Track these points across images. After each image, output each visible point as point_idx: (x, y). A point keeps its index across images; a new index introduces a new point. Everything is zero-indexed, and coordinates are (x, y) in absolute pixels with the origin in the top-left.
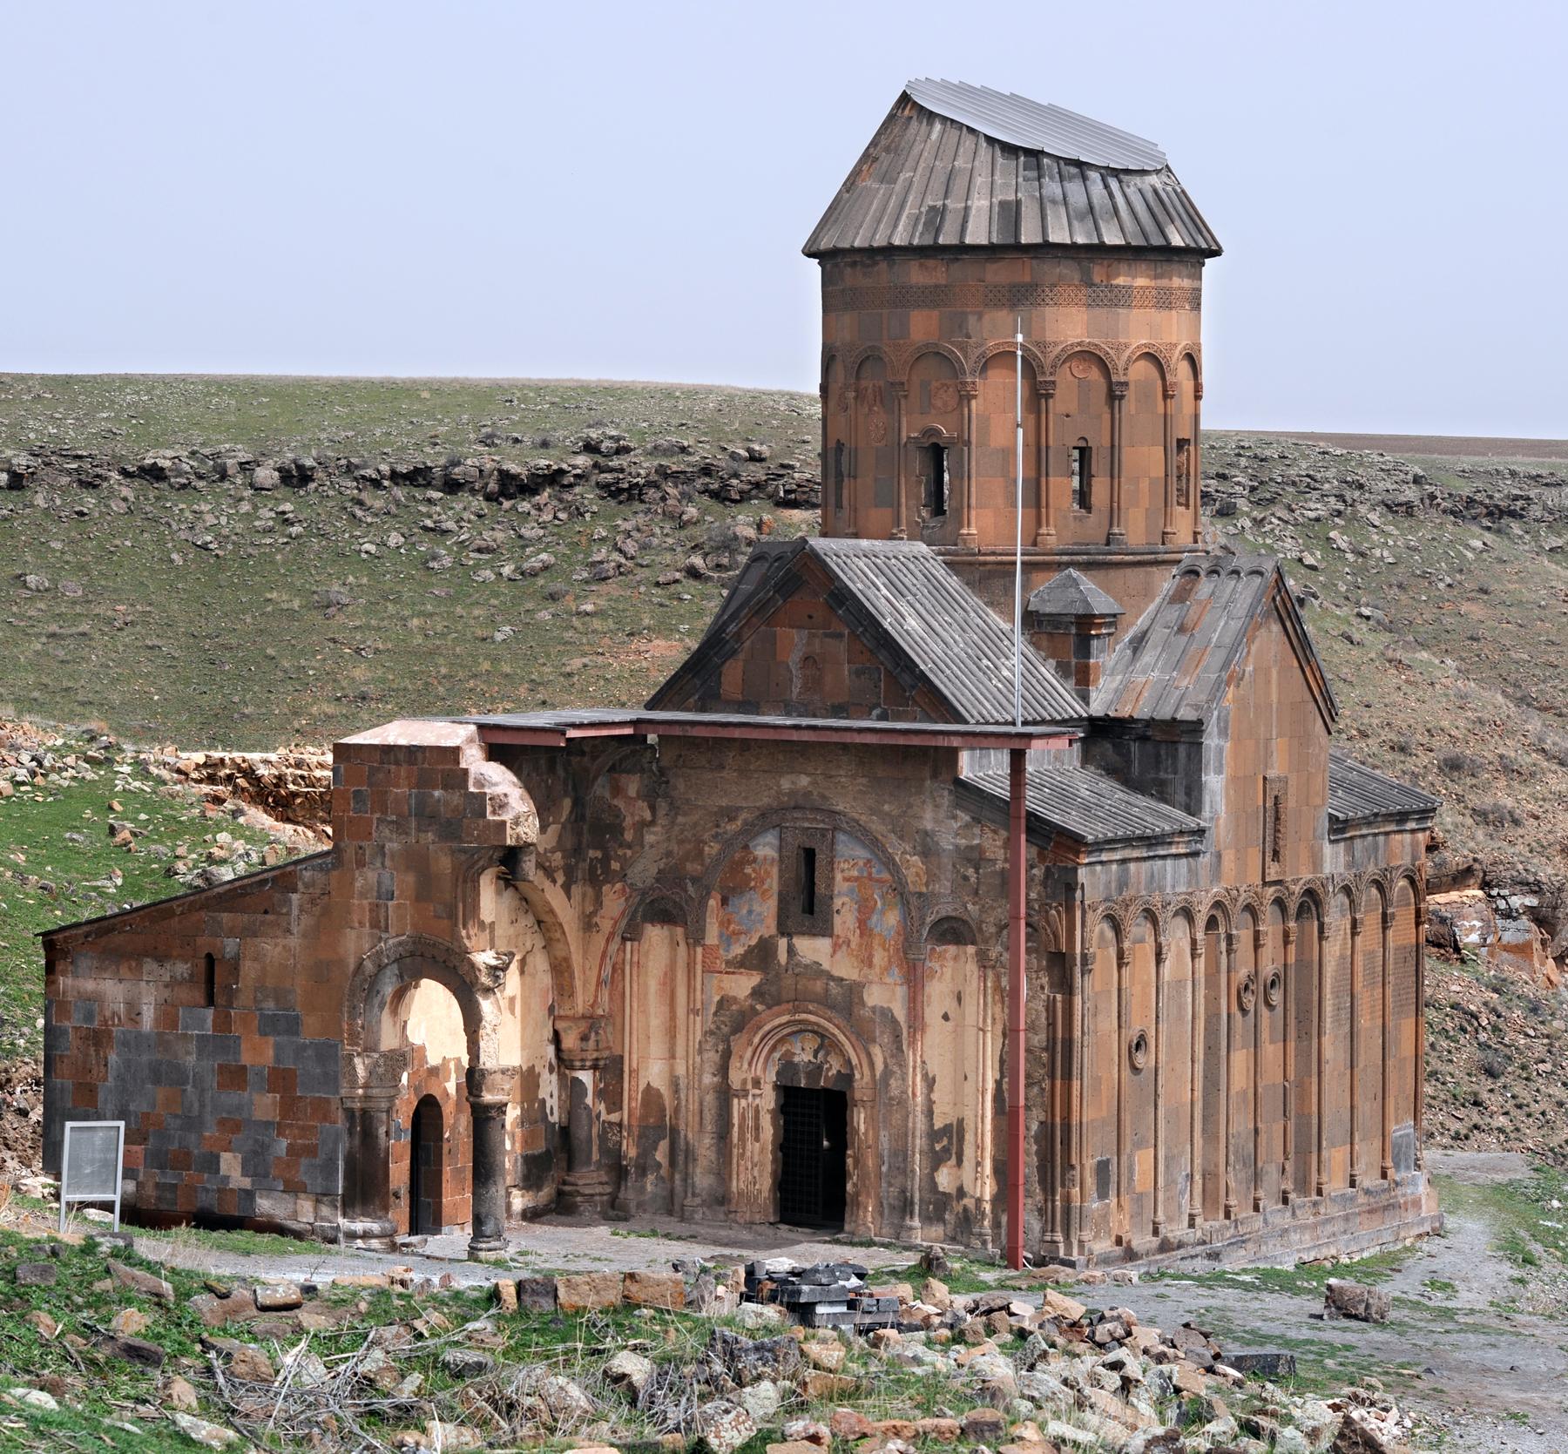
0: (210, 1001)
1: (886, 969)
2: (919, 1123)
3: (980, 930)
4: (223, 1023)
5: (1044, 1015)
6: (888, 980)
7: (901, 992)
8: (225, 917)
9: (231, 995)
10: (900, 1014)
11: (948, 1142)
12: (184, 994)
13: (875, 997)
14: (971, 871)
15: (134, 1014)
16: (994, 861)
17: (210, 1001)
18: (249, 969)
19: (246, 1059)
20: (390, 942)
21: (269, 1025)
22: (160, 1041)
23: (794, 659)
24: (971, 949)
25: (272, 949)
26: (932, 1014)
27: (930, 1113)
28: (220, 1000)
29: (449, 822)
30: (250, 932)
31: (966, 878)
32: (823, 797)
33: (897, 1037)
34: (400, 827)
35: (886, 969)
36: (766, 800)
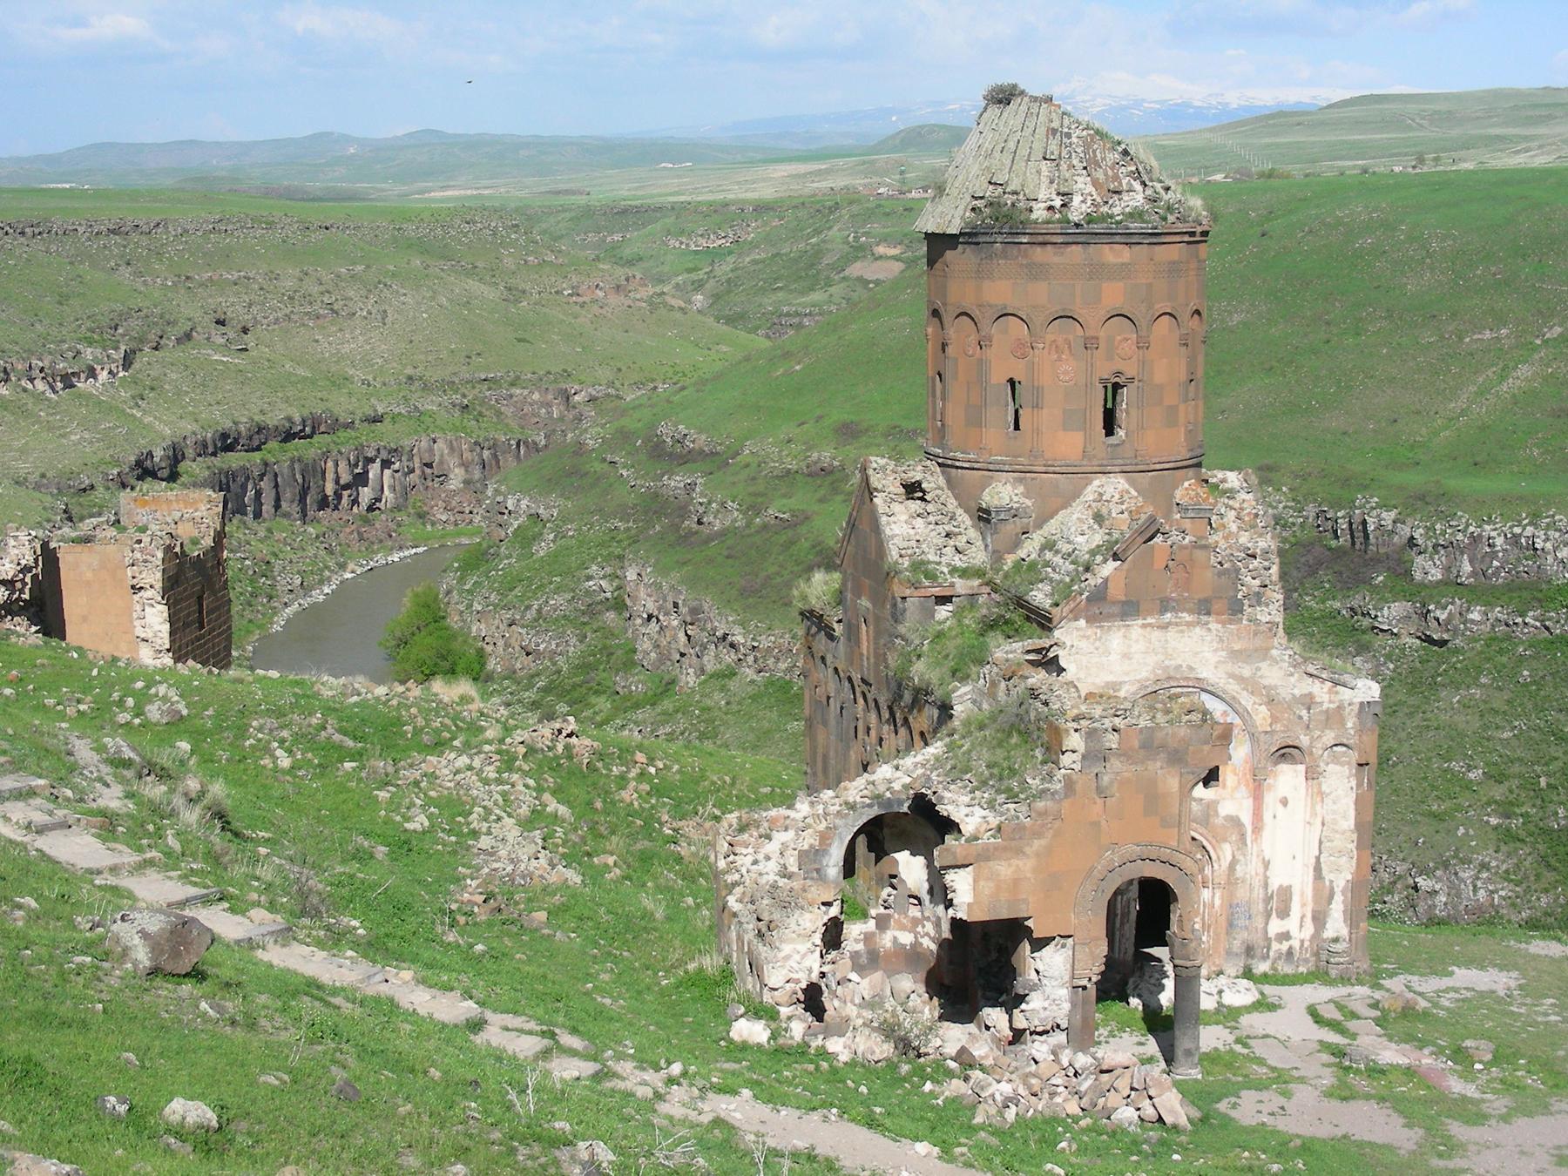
1: (1236, 788)
2: (1259, 893)
3: (1311, 753)
5: (1352, 806)
6: (1238, 795)
7: (1248, 804)
10: (1246, 819)
11: (1281, 903)
13: (1226, 809)
14: (1304, 713)
16: (1321, 703)
24: (1301, 768)
26: (1267, 816)
27: (1266, 886)
29: (1176, 751)
31: (1300, 718)
32: (1191, 668)
33: (1243, 836)
35: (1236, 788)
36: (1144, 674)
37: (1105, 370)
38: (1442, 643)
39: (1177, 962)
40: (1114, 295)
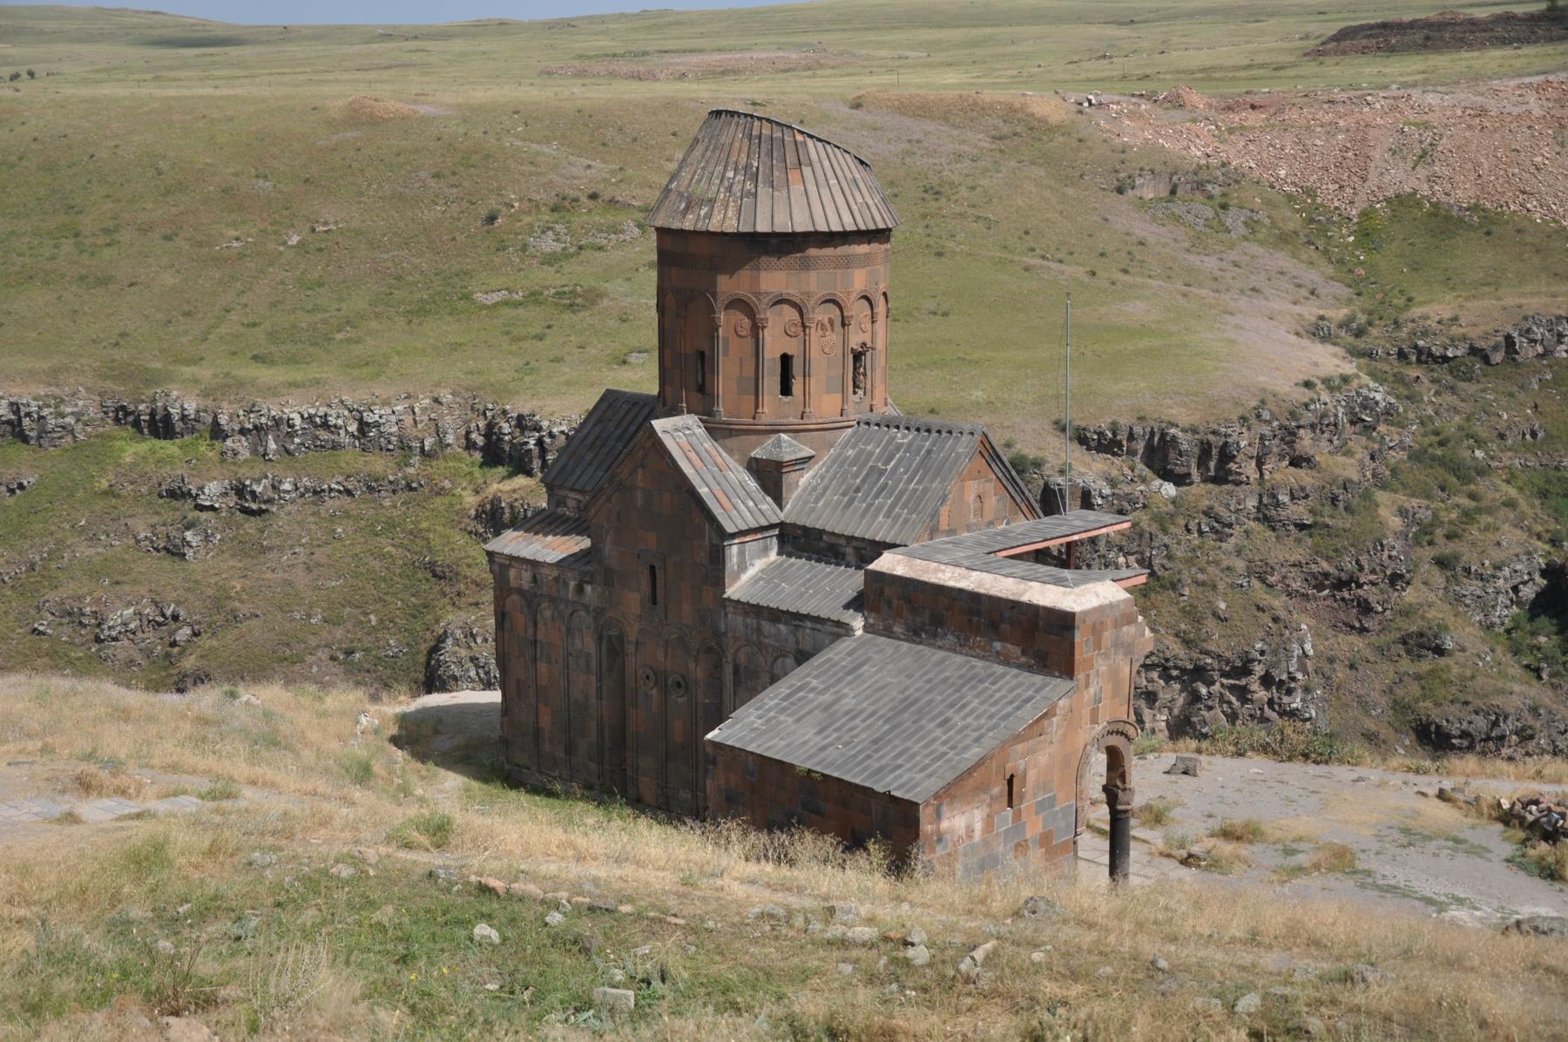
0: (1010, 804)
4: (1017, 816)
8: (1020, 747)
9: (1022, 797)
12: (996, 807)
15: (970, 831)
17: (1010, 804)
18: (1032, 775)
19: (1028, 836)
20: (1098, 728)
21: (1041, 807)
22: (985, 843)
23: (971, 497)
25: (1042, 758)
28: (1015, 802)
30: (1031, 752)
34: (1106, 656)
37: (855, 341)
38: (260, 512)
39: (1120, 807)
40: (859, 280)
